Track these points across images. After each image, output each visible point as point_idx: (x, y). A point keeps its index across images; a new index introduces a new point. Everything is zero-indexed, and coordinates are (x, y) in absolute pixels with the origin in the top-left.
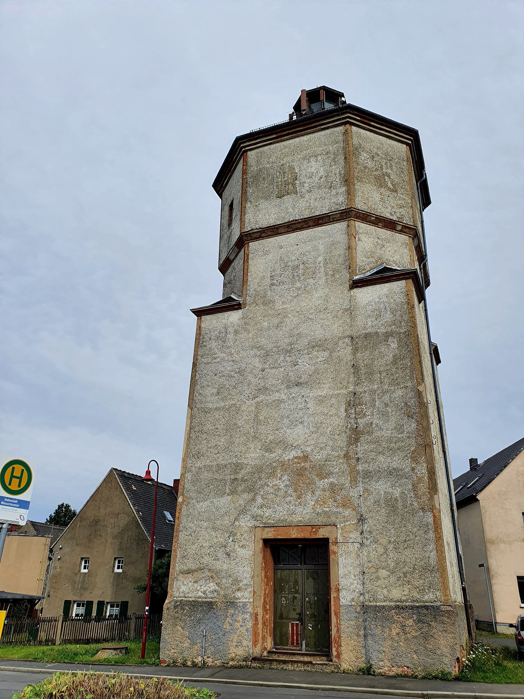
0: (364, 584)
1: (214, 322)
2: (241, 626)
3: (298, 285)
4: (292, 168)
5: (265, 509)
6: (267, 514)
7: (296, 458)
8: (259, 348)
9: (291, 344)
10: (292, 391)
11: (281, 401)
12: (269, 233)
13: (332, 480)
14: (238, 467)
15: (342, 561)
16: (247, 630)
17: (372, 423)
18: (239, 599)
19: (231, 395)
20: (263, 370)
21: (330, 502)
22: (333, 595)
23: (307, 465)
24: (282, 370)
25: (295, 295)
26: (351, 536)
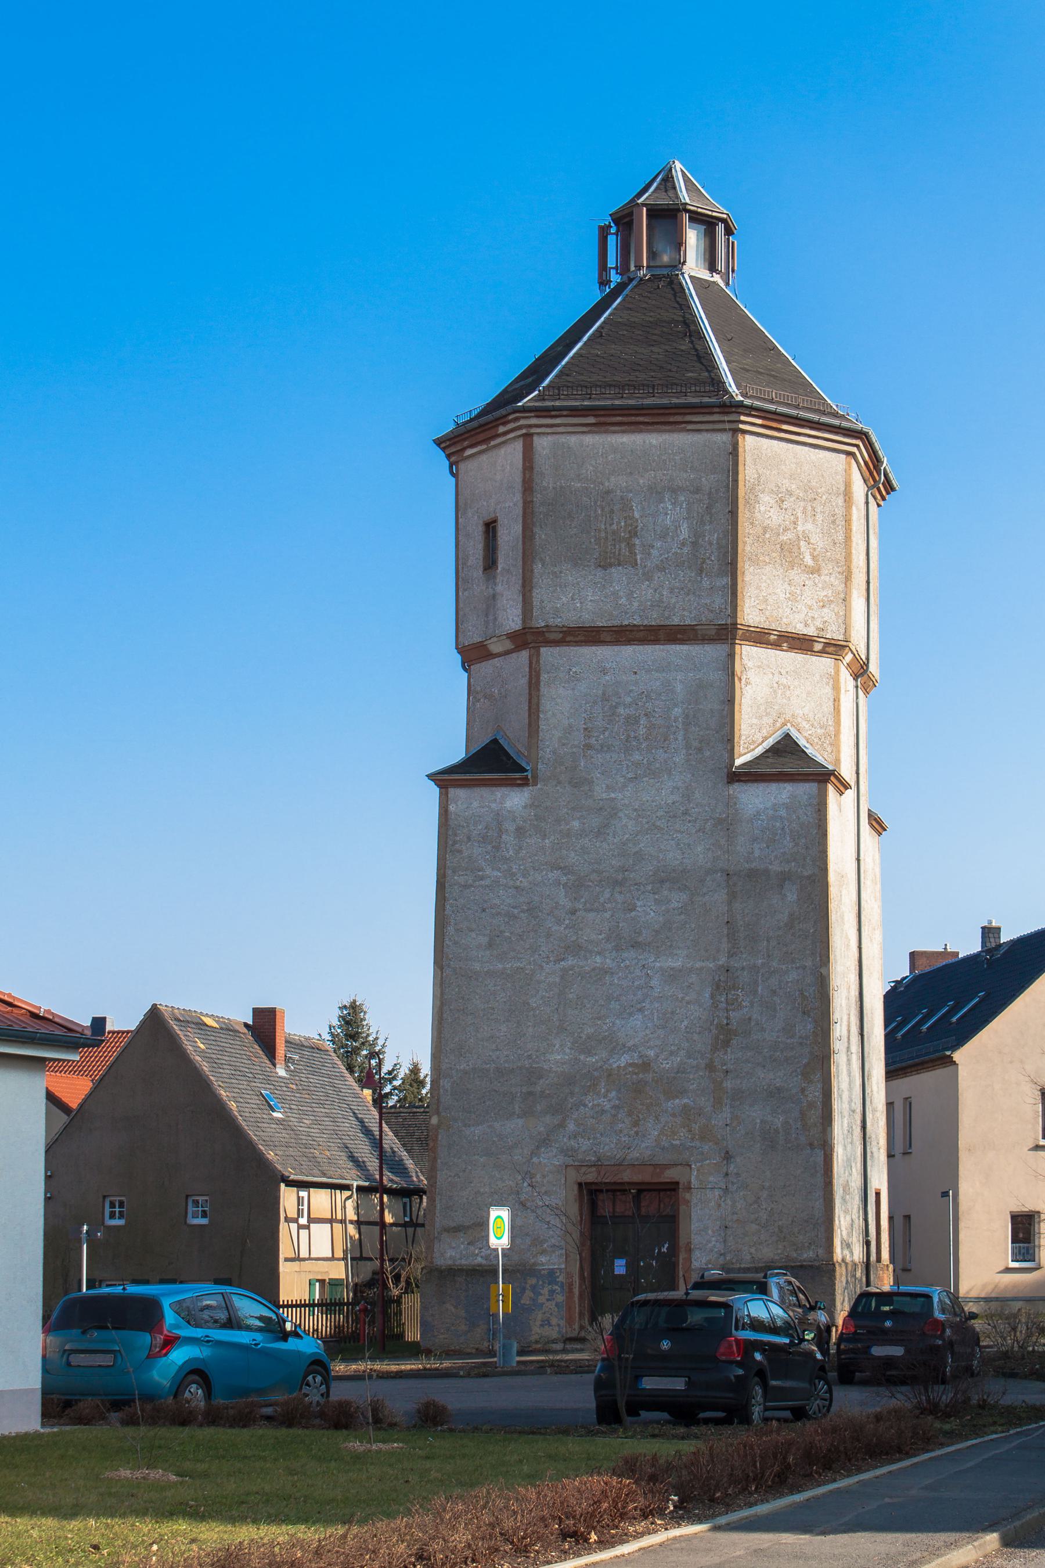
0: (725, 1241)
1: (475, 804)
2: (548, 1300)
3: (637, 757)
4: (626, 506)
5: (581, 1140)
6: (584, 1148)
7: (631, 1065)
8: (566, 870)
9: (624, 869)
10: (625, 955)
11: (606, 971)
12: (580, 638)
13: (686, 1101)
14: (534, 1074)
15: (696, 1212)
16: (557, 1305)
17: (750, 1019)
18: (543, 1264)
19: (514, 950)
20: (573, 912)
21: (683, 1133)
22: (682, 1256)
23: (649, 1077)
24: (607, 915)
25: (629, 776)
26: (711, 1179)
